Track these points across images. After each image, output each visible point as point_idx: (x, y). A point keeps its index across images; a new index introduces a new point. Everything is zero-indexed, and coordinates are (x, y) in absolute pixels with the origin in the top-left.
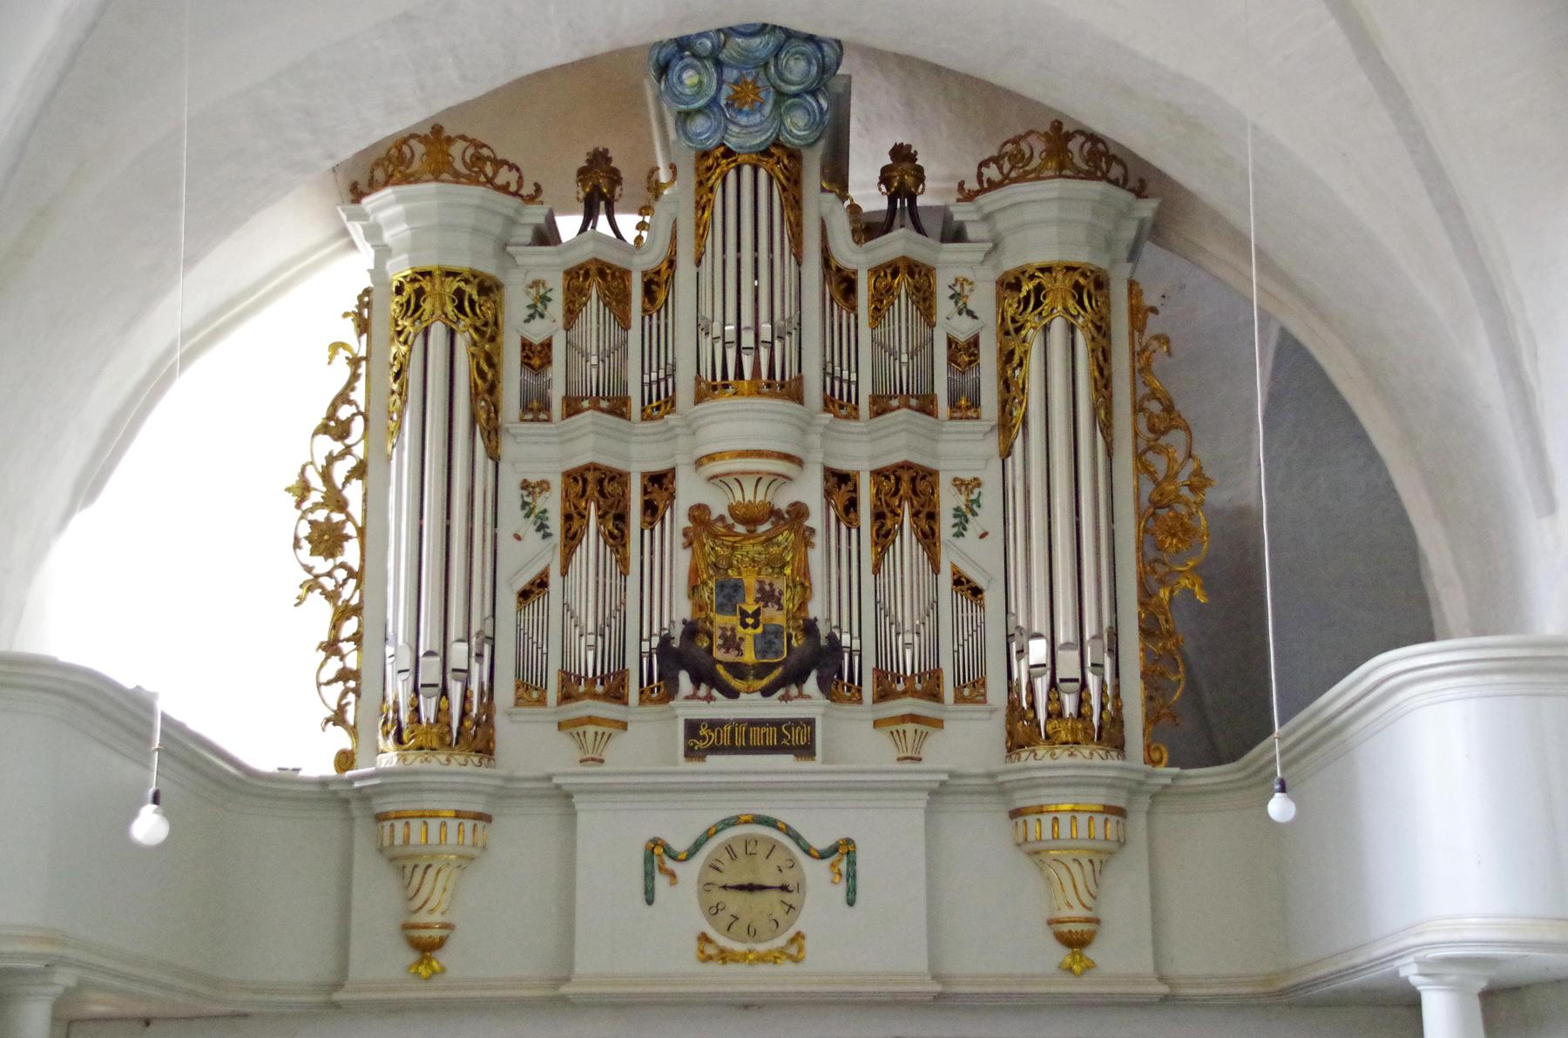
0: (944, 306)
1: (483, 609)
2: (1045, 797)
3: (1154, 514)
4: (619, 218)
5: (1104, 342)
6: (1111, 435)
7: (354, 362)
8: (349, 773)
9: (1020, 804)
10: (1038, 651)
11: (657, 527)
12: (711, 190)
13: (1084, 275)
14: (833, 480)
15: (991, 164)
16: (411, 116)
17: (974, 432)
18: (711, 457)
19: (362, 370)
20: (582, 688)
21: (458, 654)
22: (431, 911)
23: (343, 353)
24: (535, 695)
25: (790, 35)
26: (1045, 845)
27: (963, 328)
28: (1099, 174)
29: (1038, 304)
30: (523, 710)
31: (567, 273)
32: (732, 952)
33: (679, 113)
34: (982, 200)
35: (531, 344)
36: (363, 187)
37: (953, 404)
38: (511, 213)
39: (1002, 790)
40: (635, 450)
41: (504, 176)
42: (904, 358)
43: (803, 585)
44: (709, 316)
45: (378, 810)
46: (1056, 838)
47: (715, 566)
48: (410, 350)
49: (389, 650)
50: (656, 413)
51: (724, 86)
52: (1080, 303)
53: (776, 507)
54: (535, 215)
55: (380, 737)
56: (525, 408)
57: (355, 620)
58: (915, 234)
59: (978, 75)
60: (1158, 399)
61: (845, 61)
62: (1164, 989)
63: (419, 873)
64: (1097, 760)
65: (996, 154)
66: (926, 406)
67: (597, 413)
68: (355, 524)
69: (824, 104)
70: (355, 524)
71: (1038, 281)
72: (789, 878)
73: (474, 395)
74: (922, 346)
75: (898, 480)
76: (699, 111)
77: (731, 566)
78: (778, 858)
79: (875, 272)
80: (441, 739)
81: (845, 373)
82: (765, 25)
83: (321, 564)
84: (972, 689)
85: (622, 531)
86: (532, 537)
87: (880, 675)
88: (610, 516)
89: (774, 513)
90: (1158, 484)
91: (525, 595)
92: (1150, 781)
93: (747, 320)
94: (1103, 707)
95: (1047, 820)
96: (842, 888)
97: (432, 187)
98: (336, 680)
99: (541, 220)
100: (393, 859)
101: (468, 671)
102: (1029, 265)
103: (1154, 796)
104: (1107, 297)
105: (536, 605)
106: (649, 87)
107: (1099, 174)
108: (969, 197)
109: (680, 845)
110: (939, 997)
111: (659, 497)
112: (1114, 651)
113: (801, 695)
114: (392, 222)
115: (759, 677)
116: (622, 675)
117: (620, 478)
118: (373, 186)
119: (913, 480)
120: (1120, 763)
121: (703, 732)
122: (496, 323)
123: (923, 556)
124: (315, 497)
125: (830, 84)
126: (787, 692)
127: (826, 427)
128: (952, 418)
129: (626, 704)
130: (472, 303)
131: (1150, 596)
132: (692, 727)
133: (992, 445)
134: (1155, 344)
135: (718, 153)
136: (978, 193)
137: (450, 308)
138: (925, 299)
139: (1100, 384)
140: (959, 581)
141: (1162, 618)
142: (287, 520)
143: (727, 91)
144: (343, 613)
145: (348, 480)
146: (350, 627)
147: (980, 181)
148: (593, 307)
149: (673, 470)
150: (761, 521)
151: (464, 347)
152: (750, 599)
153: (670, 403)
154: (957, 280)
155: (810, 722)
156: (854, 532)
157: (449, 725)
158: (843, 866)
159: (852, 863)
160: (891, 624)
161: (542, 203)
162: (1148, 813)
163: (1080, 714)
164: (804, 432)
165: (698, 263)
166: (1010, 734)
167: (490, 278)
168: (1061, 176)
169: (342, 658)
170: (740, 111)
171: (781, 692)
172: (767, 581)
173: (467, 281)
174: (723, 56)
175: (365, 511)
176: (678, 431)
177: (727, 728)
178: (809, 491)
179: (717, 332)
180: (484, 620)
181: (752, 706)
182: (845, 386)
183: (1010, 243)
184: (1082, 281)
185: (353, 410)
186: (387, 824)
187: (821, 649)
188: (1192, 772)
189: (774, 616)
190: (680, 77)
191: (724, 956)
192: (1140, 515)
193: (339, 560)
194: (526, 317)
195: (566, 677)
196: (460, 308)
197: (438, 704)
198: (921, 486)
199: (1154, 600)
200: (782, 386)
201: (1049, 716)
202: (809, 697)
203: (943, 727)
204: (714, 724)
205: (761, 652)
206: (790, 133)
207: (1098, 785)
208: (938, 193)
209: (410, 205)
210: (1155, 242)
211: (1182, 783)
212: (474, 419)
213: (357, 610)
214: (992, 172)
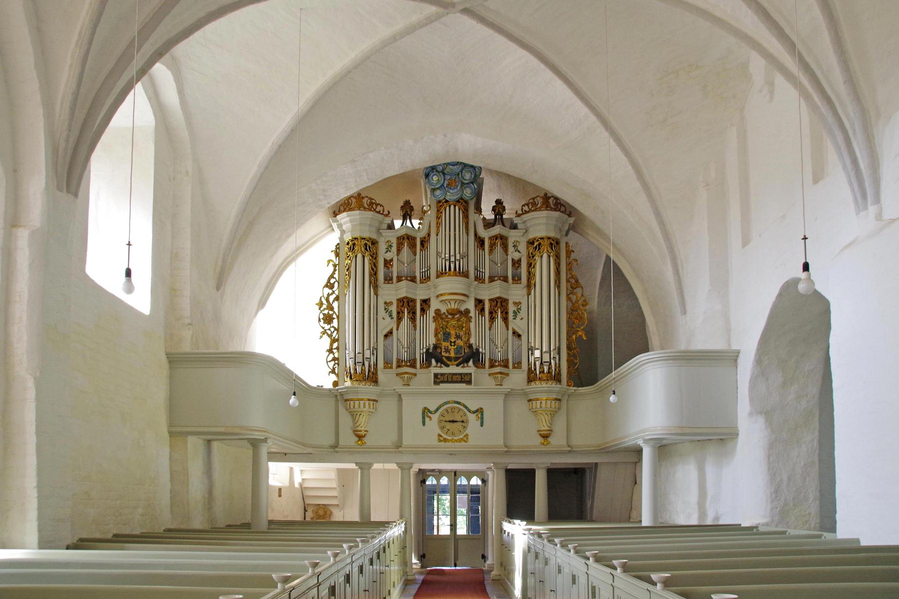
0: (511, 249)
1: (374, 341)
2: (538, 396)
3: (572, 313)
4: (413, 221)
5: (558, 260)
6: (560, 289)
7: (335, 266)
8: (337, 388)
9: (531, 398)
10: (537, 353)
11: (425, 316)
12: (441, 213)
13: (553, 240)
14: (477, 302)
15: (526, 206)
16: (353, 191)
17: (519, 288)
18: (441, 295)
19: (337, 268)
20: (403, 364)
21: (367, 354)
22: (362, 427)
23: (331, 263)
24: (389, 365)
25: (465, 166)
26: (537, 409)
27: (516, 256)
28: (558, 209)
29: (539, 249)
30: (386, 370)
31: (398, 238)
32: (448, 439)
33: (432, 189)
34: (523, 216)
35: (387, 260)
36: (337, 212)
37: (513, 279)
38: (381, 220)
39: (526, 394)
40: (418, 292)
41: (379, 209)
42: (499, 265)
43: (468, 334)
44: (441, 251)
45: (345, 398)
46: (541, 407)
47: (442, 327)
48: (351, 262)
49: (347, 352)
50: (424, 281)
51: (446, 181)
52: (552, 249)
53: (461, 310)
54: (388, 221)
55: (345, 377)
56: (385, 279)
57: (337, 343)
58: (502, 226)
59: (523, 178)
60: (574, 279)
61: (482, 174)
62: (569, 449)
63: (358, 416)
64: (553, 385)
65: (527, 202)
66: (505, 279)
67: (407, 281)
68: (336, 315)
69: (476, 187)
70: (336, 315)
71: (539, 242)
72: (464, 418)
73: (370, 275)
74: (504, 261)
75: (497, 302)
76: (438, 188)
77: (447, 328)
78: (461, 413)
79: (490, 238)
80: (363, 378)
81: (481, 269)
82: (458, 162)
83: (327, 327)
84: (518, 365)
85: (414, 317)
86: (388, 319)
87: (491, 360)
88: (411, 313)
89: (460, 312)
90: (573, 304)
91: (386, 336)
92: (569, 391)
93: (452, 253)
94: (555, 370)
95: (539, 402)
96: (479, 422)
97: (358, 212)
98: (332, 361)
99: (390, 222)
100: (350, 412)
101: (370, 358)
102: (537, 237)
103: (569, 396)
104: (559, 247)
105: (389, 339)
106: (422, 181)
107: (558, 209)
108: (518, 216)
109: (432, 409)
110: (506, 452)
111: (425, 307)
112: (559, 353)
113: (468, 366)
114: (345, 223)
115: (455, 361)
116: (415, 360)
117: (414, 301)
118: (340, 212)
119: (501, 302)
120: (560, 386)
121: (439, 377)
122: (376, 253)
123: (504, 325)
124: (324, 306)
125: (478, 180)
126: (464, 365)
127: (476, 286)
128: (513, 283)
129: (416, 368)
130: (369, 247)
131: (570, 337)
132: (436, 375)
133: (525, 291)
134: (573, 261)
135: (443, 201)
136: (521, 214)
137: (363, 249)
138: (505, 247)
139: (557, 274)
140: (514, 333)
141: (573, 344)
142: (316, 313)
143: (446, 182)
144: (333, 341)
145: (334, 301)
146: (335, 345)
147: (522, 211)
148: (406, 248)
149: (429, 299)
150: (456, 315)
151: (367, 262)
152: (453, 338)
153: (429, 278)
154: (515, 241)
155: (471, 374)
156: (483, 318)
157: (365, 374)
158: (480, 415)
159: (482, 415)
160: (494, 345)
161: (390, 217)
162: (567, 400)
163: (549, 372)
164: (469, 287)
165: (437, 235)
166: (528, 378)
167: (375, 240)
168: (547, 210)
169: (334, 355)
170: (451, 189)
171: (462, 365)
172: (458, 332)
173: (368, 241)
174: (445, 172)
175: (339, 311)
176: (431, 287)
177: (446, 376)
178: (470, 305)
179: (443, 256)
180: (374, 343)
181: (453, 369)
182: (481, 273)
183: (531, 229)
184: (552, 242)
185: (335, 280)
186: (348, 402)
187: (474, 353)
188: (580, 388)
189: (460, 342)
190: (432, 178)
191: (445, 440)
192: (567, 313)
193: (332, 325)
194: (385, 252)
195: (398, 361)
196: (366, 249)
197: (362, 368)
198: (504, 304)
199: (571, 338)
200: (463, 273)
201: (540, 372)
202: (470, 367)
203: (508, 375)
204: (442, 375)
205: (456, 353)
206: (465, 195)
207: (554, 392)
208: (509, 214)
209: (351, 218)
210: (573, 231)
211: (577, 392)
212: (370, 283)
213: (337, 340)
214: (526, 208)
